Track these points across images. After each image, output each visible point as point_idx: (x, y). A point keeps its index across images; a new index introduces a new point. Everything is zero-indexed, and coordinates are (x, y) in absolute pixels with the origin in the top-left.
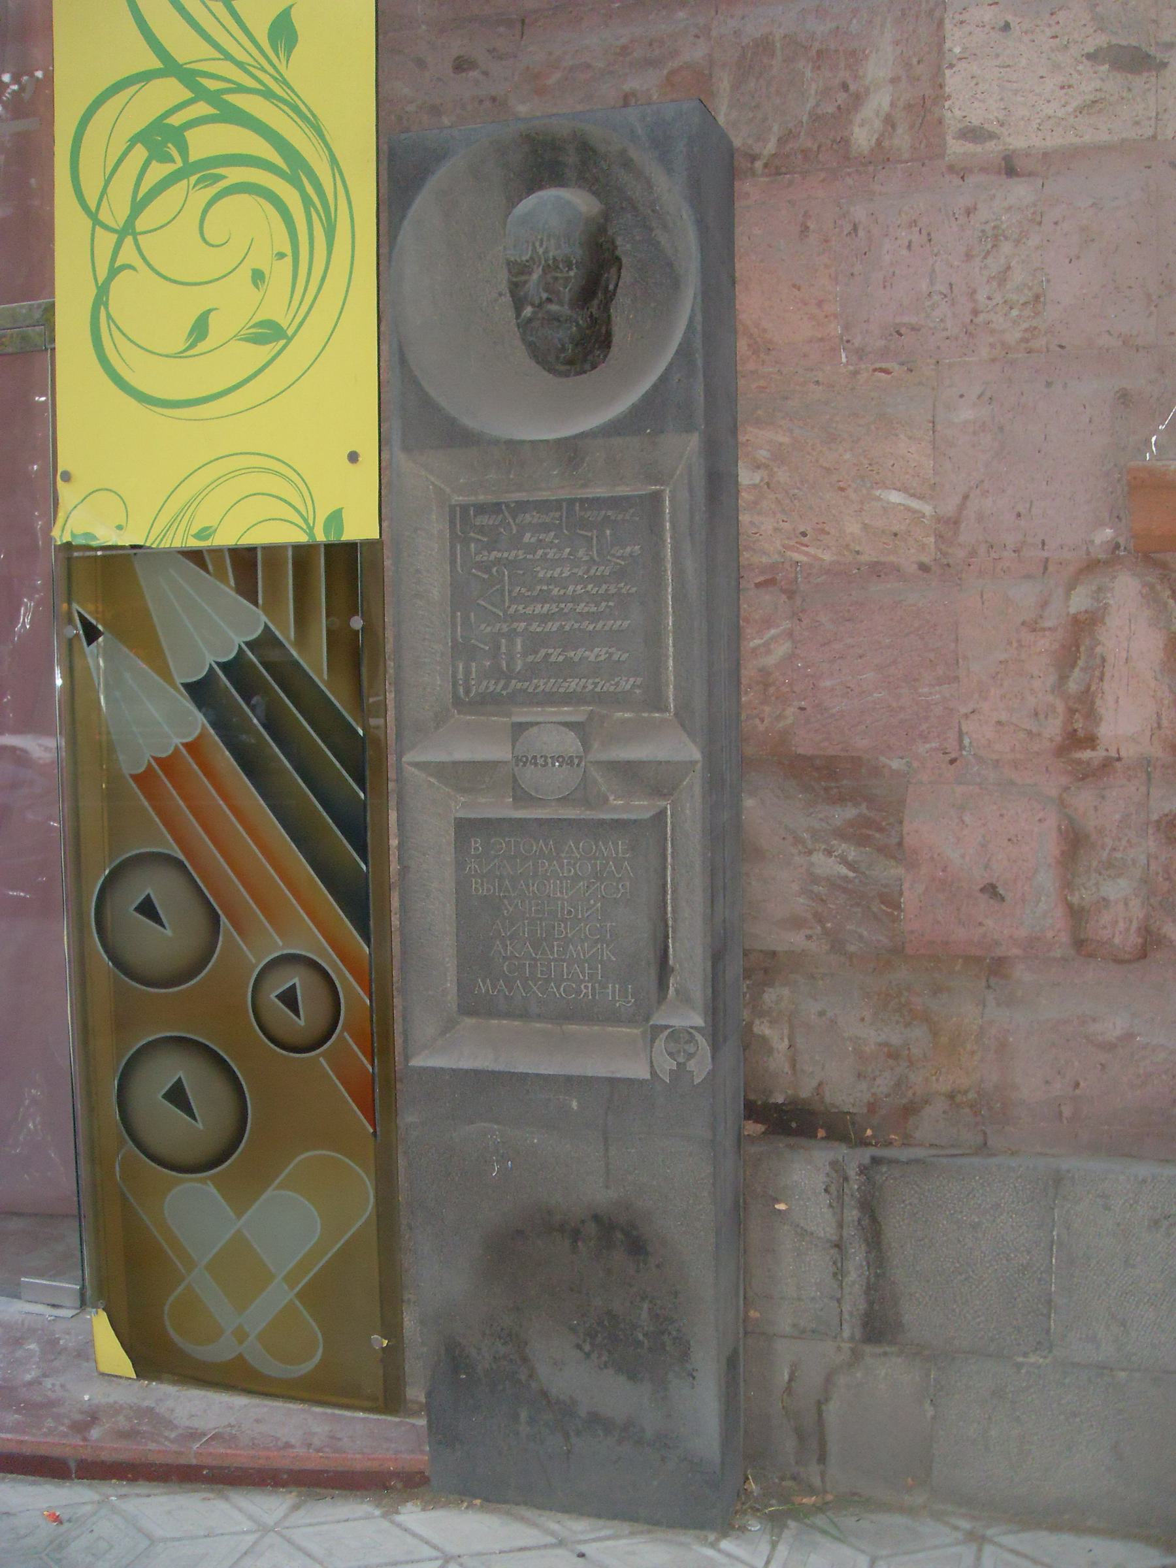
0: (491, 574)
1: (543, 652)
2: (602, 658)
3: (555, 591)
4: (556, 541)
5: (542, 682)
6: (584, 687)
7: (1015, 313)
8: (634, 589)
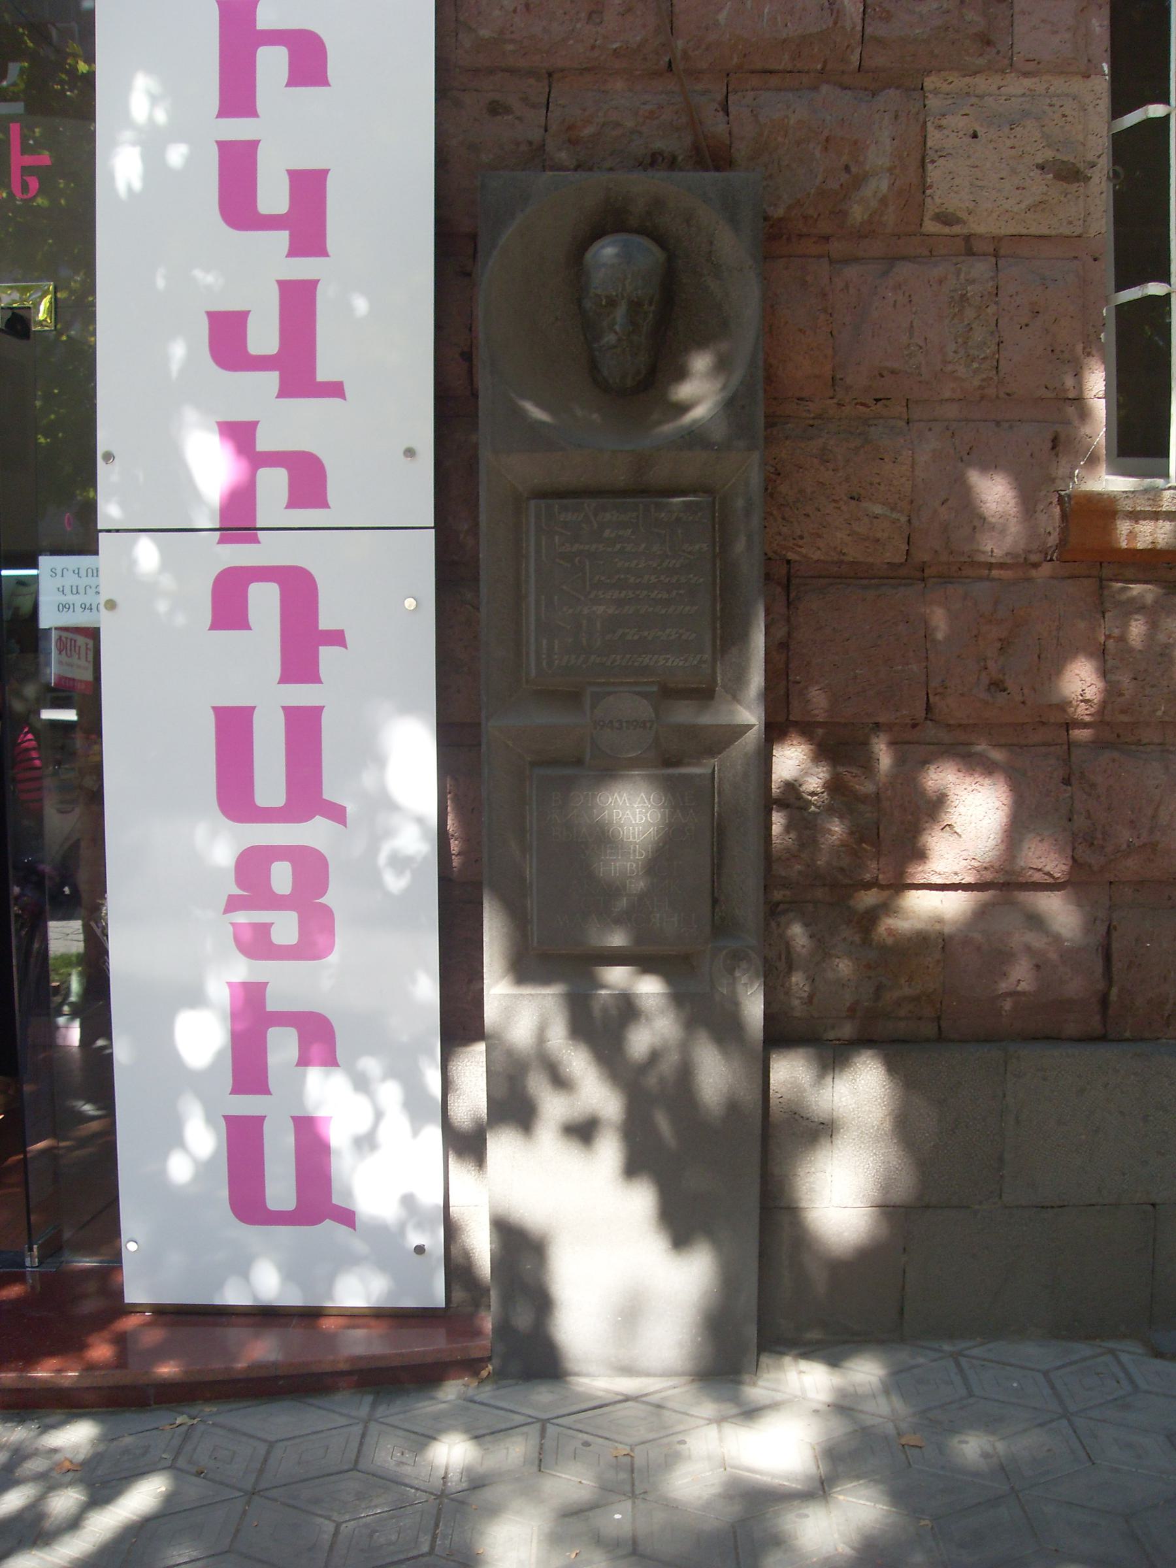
1: (620, 632)
2: (673, 637)
3: (632, 580)
6: (656, 662)
7: (975, 365)
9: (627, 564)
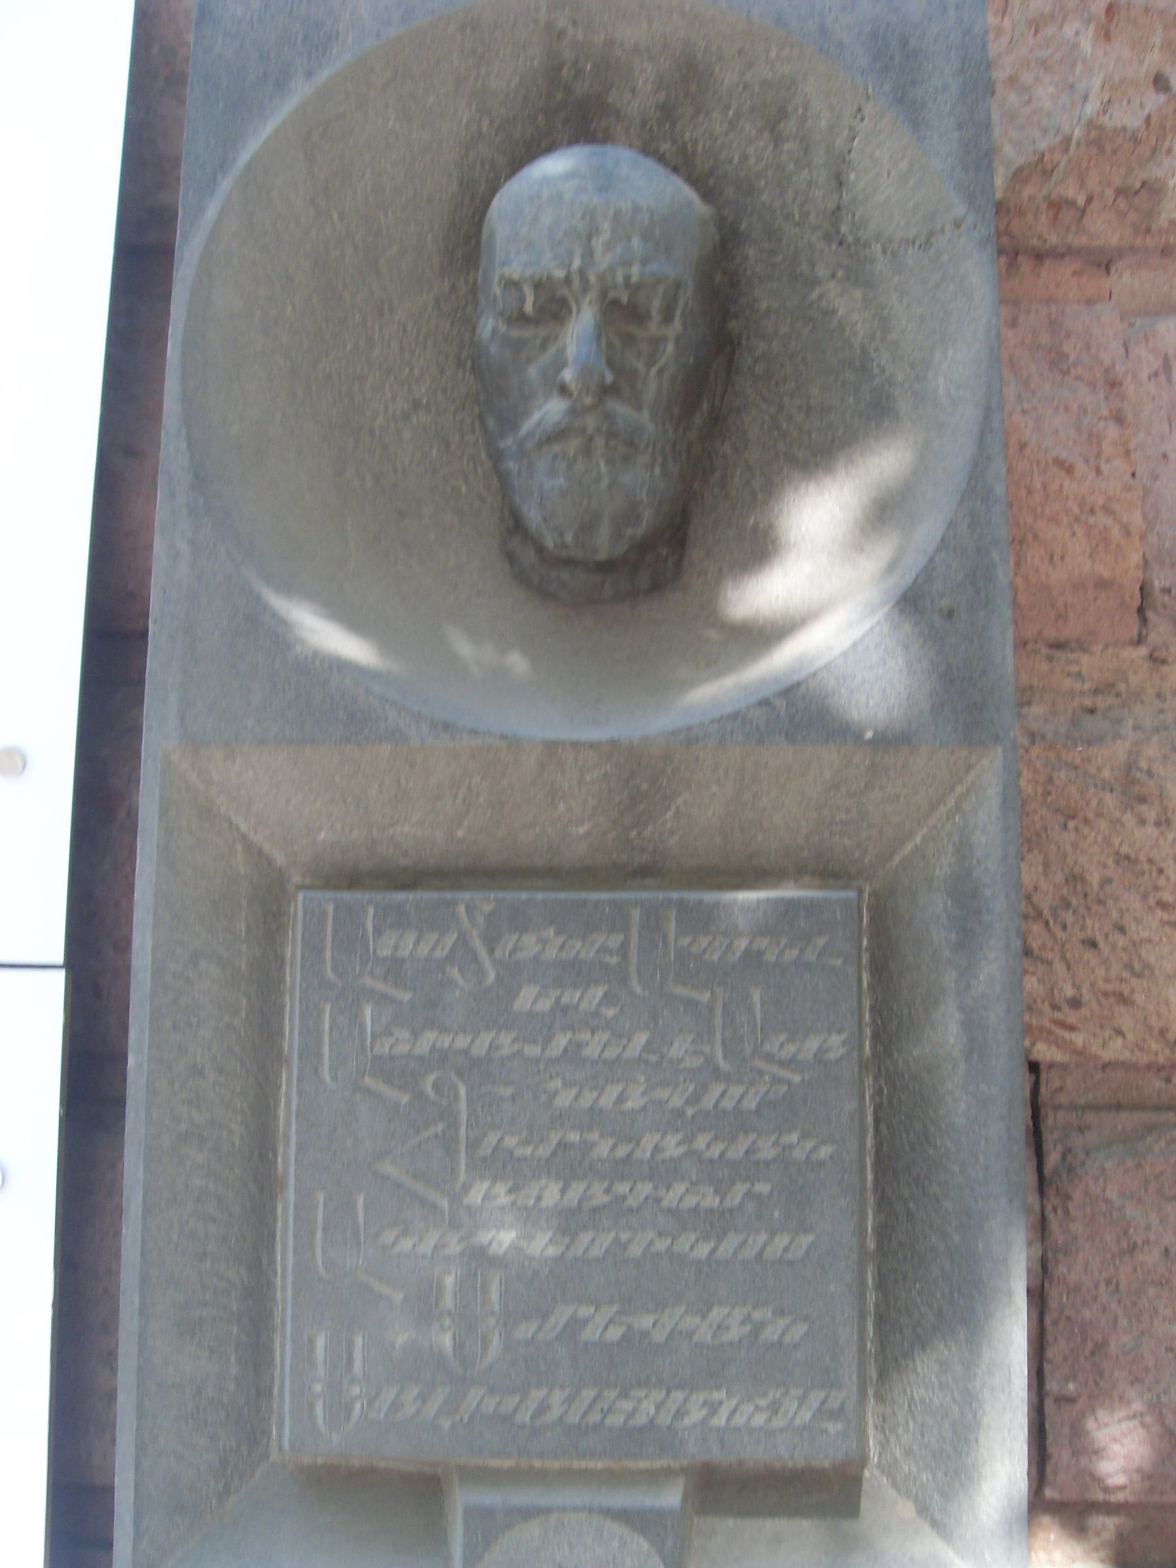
0: (419, 1096)
1: (562, 1314)
2: (733, 1335)
3: (603, 1149)
4: (610, 1012)
5: (557, 1397)
6: (680, 1414)
8: (825, 1152)
9: (587, 1099)
